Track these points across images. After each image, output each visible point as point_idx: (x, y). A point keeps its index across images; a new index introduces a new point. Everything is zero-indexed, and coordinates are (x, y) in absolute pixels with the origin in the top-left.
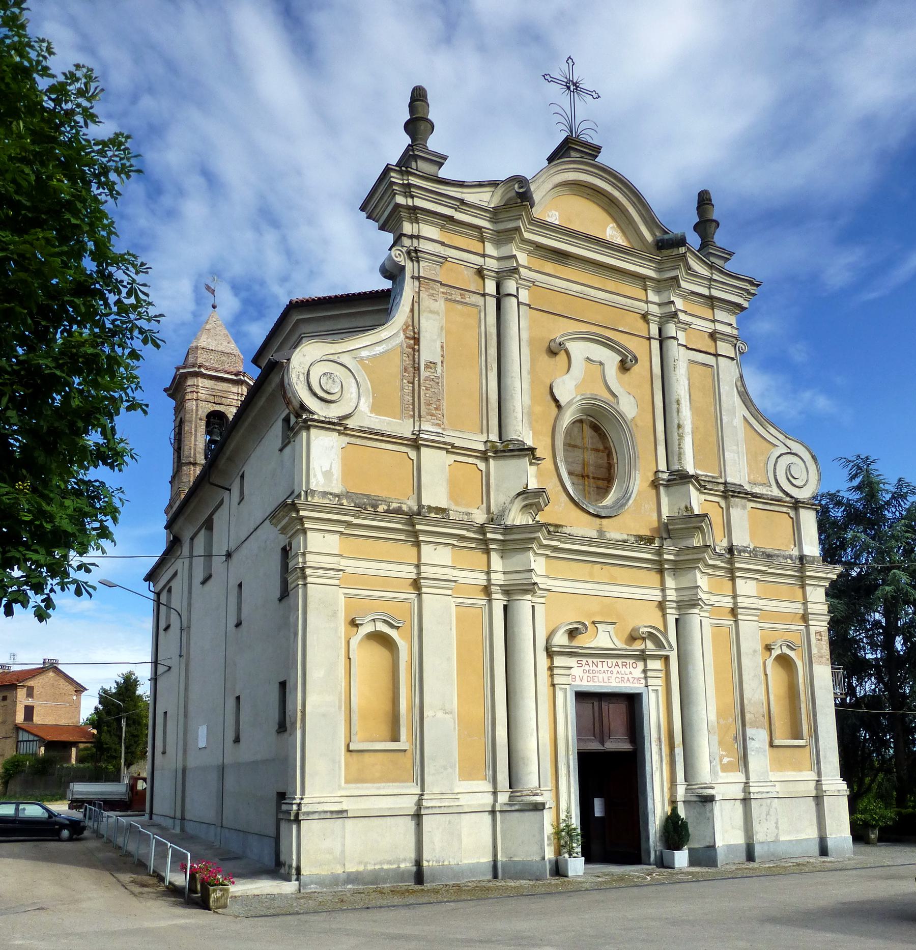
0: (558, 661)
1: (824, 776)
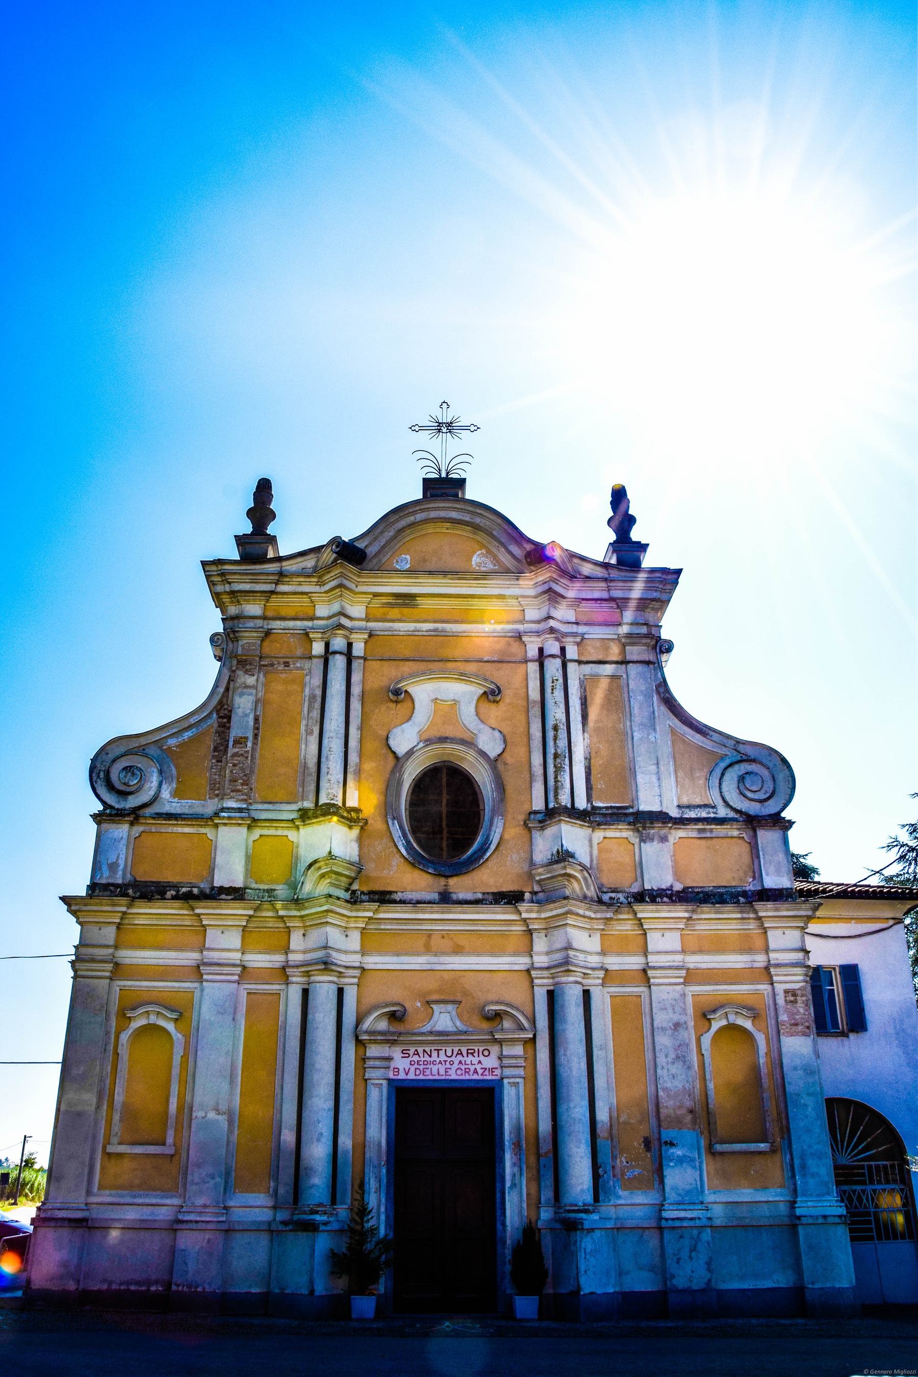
0: (373, 1051)
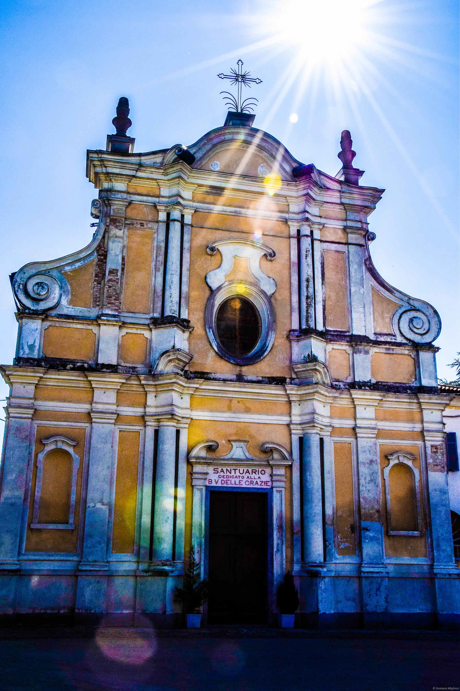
0: (197, 469)
1: (437, 562)
